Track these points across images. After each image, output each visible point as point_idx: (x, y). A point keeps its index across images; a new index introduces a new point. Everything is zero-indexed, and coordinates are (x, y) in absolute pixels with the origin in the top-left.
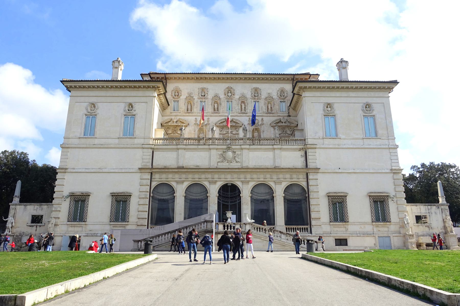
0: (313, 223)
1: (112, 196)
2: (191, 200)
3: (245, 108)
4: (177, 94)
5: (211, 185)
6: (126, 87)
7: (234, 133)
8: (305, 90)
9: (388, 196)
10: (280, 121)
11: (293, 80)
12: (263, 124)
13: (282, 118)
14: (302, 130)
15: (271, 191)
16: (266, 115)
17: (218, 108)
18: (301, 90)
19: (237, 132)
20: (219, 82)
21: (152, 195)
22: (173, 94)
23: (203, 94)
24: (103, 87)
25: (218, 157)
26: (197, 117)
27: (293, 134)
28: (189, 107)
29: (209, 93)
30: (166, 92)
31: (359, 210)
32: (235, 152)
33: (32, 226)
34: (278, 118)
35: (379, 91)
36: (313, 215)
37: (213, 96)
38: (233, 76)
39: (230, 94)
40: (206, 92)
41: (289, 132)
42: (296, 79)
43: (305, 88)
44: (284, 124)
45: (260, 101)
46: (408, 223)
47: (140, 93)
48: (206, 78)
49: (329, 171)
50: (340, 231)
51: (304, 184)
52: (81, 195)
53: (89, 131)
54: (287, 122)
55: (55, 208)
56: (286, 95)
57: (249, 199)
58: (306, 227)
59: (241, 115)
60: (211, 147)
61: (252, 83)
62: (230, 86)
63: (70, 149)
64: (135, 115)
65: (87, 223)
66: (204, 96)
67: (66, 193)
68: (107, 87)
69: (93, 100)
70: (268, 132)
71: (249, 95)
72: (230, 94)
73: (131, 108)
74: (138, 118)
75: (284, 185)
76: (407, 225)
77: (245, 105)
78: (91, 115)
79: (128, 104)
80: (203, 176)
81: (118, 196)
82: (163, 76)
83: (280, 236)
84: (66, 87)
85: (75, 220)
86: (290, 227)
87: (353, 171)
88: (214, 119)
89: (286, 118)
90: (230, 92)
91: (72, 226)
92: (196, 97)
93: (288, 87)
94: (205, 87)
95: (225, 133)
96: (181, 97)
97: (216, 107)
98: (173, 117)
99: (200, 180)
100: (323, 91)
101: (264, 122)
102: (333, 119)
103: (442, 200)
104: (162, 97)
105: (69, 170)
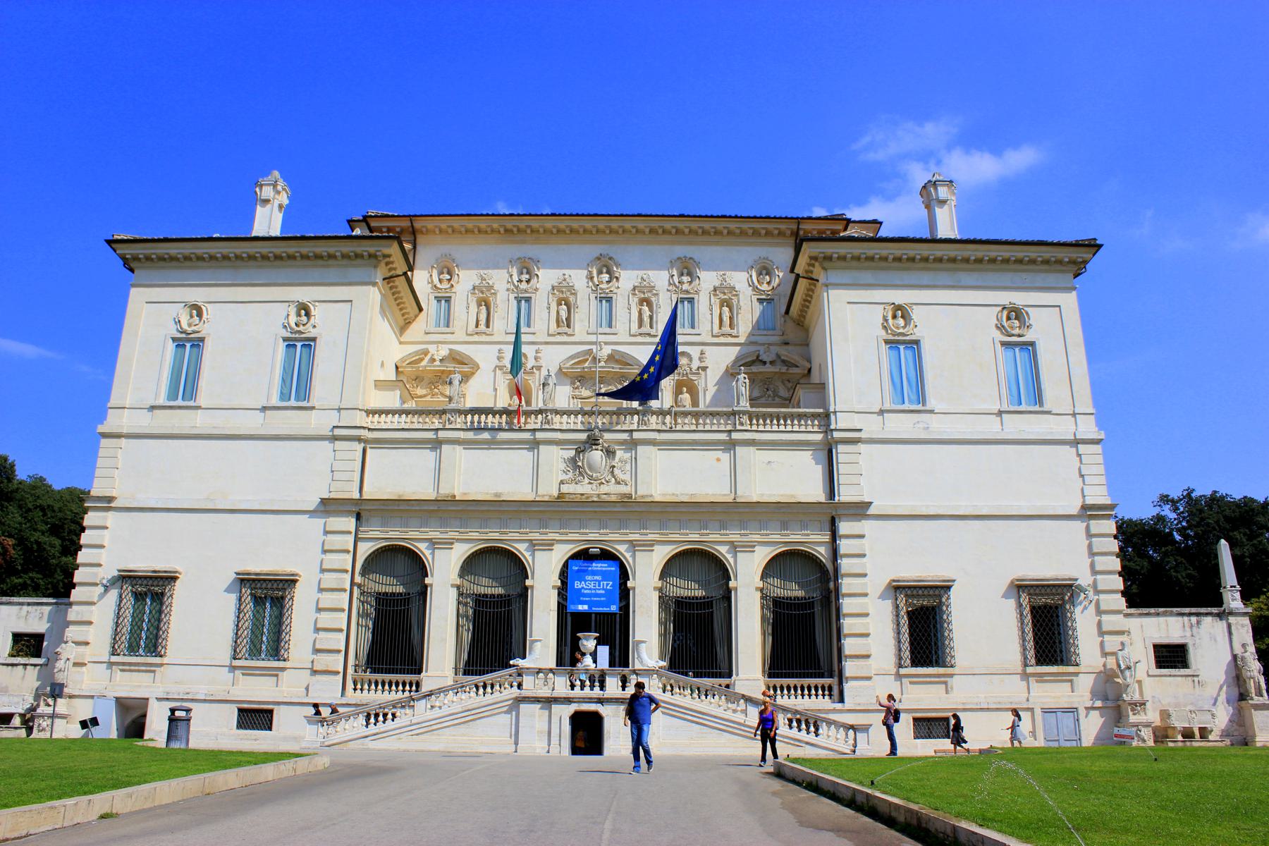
0: (850, 668)
1: (242, 580)
3: (651, 317)
8: (826, 264)
9: (1071, 586)
11: (796, 234)
13: (762, 349)
14: (822, 387)
17: (568, 319)
18: (817, 264)
21: (358, 579)
25: (563, 466)
26: (502, 346)
31: (985, 630)
32: (614, 453)
33: (13, 665)
34: (753, 348)
35: (1046, 271)
36: (849, 645)
43: (829, 258)
45: (696, 297)
46: (1129, 668)
50: (923, 695)
51: (822, 552)
52: (151, 578)
54: (779, 362)
55: (78, 613)
57: (656, 595)
58: (826, 681)
59: (639, 339)
60: (539, 435)
61: (673, 243)
62: (604, 252)
63: (123, 440)
64: (314, 339)
65: (165, 660)
66: (528, 281)
67: (108, 572)
68: (238, 257)
73: (304, 319)
74: (321, 350)
76: (1127, 673)
77: (651, 310)
81: (259, 580)
82: (405, 223)
83: (742, 711)
84: (123, 258)
85: (133, 649)
86: (778, 681)
89: (774, 349)
91: (127, 667)
96: (457, 288)
97: (564, 314)
98: (432, 348)
100: (882, 269)
102: (909, 353)
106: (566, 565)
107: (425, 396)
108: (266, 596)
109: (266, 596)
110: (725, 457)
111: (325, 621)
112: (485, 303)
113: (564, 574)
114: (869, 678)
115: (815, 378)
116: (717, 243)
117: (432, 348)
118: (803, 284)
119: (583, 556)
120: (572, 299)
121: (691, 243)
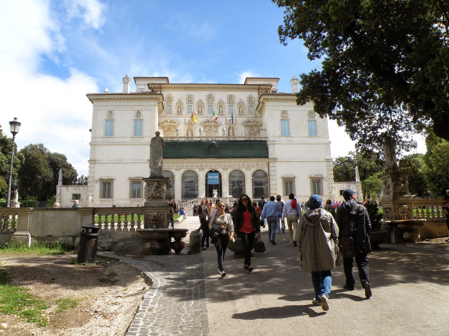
2: (186, 182)
4: (169, 100)
6: (135, 99)
10: (249, 121)
11: (259, 89)
15: (243, 175)
16: (238, 116)
20: (202, 91)
23: (190, 99)
24: (117, 99)
27: (259, 132)
28: (179, 110)
29: (194, 99)
30: (164, 100)
34: (248, 119)
37: (198, 101)
38: (213, 86)
39: (210, 100)
40: (192, 98)
41: (255, 130)
42: (261, 88)
43: (268, 99)
44: (252, 124)
47: (145, 103)
48: (192, 88)
49: (284, 160)
53: (109, 133)
56: (253, 100)
69: (110, 108)
71: (225, 100)
72: (210, 100)
75: (253, 170)
78: (110, 119)
79: (136, 112)
80: (194, 165)
82: (159, 86)
87: (299, 160)
89: (254, 119)
90: (210, 98)
92: (184, 102)
93: (255, 94)
94: (191, 94)
95: (207, 130)
98: (167, 118)
101: (237, 122)
103: (358, 179)
104: (161, 104)
106: (207, 174)
113: (206, 176)
115: (264, 127)
116: (239, 91)
117: (167, 118)
118: (261, 104)
119: (211, 172)
120: (202, 106)
121: (232, 91)
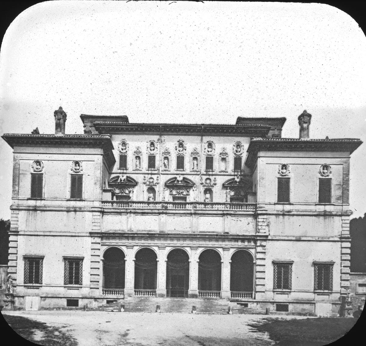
5: (160, 250)
7: (185, 193)
12: (215, 184)
19: (188, 193)
22: (121, 150)
70: (220, 195)
88: (164, 179)
99: (149, 245)
101: (217, 182)
105: (20, 233)
107: (119, 193)
108: (73, 265)
109: (73, 265)
110: (221, 218)
111: (92, 271)
112: (138, 158)
114: (264, 292)
